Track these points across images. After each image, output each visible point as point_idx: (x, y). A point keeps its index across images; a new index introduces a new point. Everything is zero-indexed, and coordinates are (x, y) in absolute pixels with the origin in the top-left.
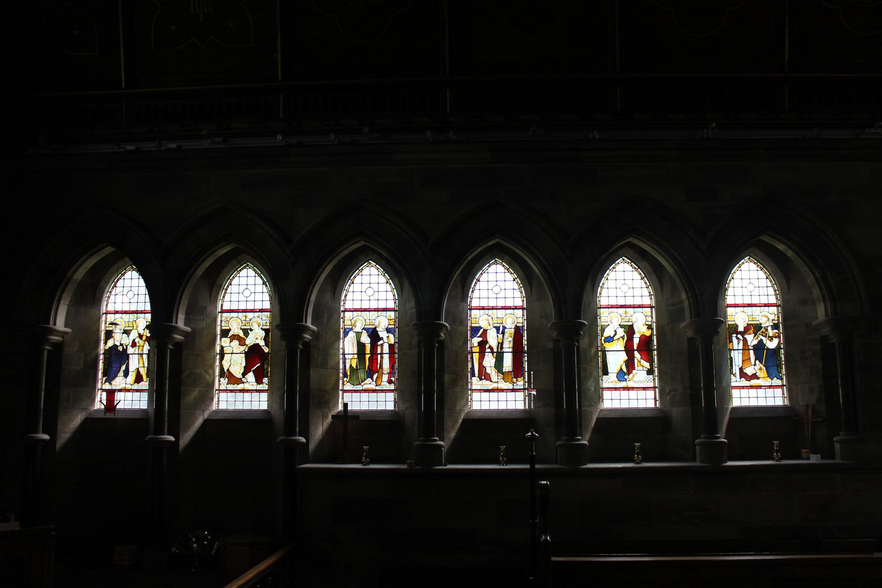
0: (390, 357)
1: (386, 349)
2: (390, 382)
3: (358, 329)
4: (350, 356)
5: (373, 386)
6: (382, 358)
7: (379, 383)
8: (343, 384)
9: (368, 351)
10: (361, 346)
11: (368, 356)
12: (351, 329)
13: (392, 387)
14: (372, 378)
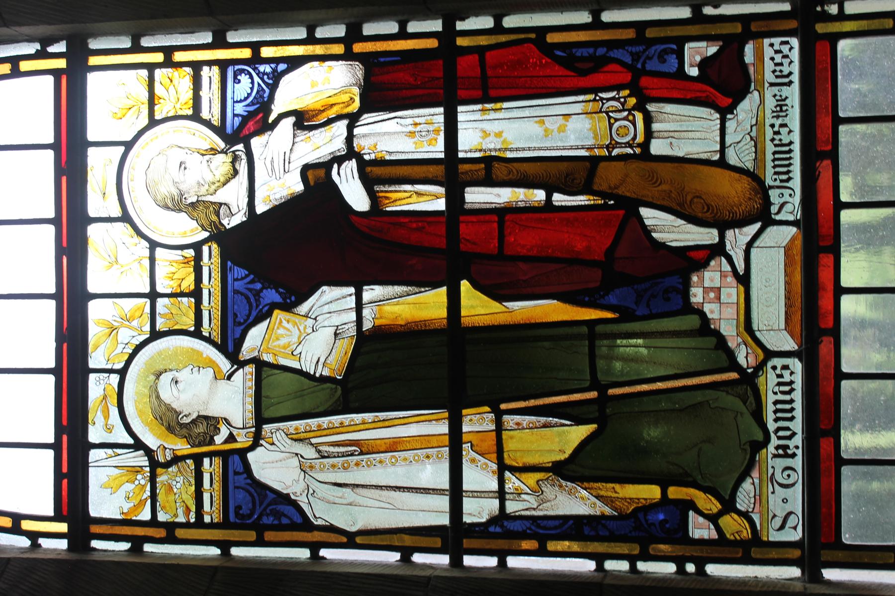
0: (491, 90)
1: (405, 134)
2: (724, 85)
3: (229, 400)
4: (478, 476)
5: (770, 256)
6: (493, 169)
7: (731, 191)
8: (752, 549)
9: (428, 305)
10: (381, 372)
11: (476, 306)
12: (235, 462)
13: (778, 58)
14: (696, 259)
